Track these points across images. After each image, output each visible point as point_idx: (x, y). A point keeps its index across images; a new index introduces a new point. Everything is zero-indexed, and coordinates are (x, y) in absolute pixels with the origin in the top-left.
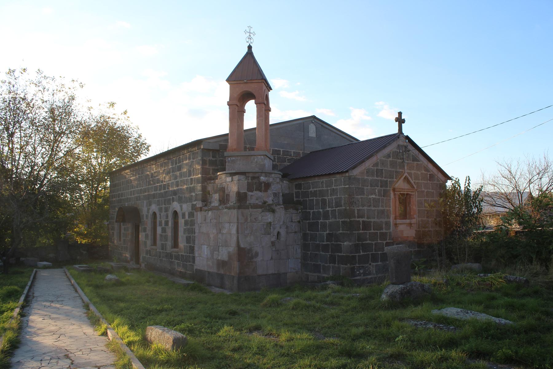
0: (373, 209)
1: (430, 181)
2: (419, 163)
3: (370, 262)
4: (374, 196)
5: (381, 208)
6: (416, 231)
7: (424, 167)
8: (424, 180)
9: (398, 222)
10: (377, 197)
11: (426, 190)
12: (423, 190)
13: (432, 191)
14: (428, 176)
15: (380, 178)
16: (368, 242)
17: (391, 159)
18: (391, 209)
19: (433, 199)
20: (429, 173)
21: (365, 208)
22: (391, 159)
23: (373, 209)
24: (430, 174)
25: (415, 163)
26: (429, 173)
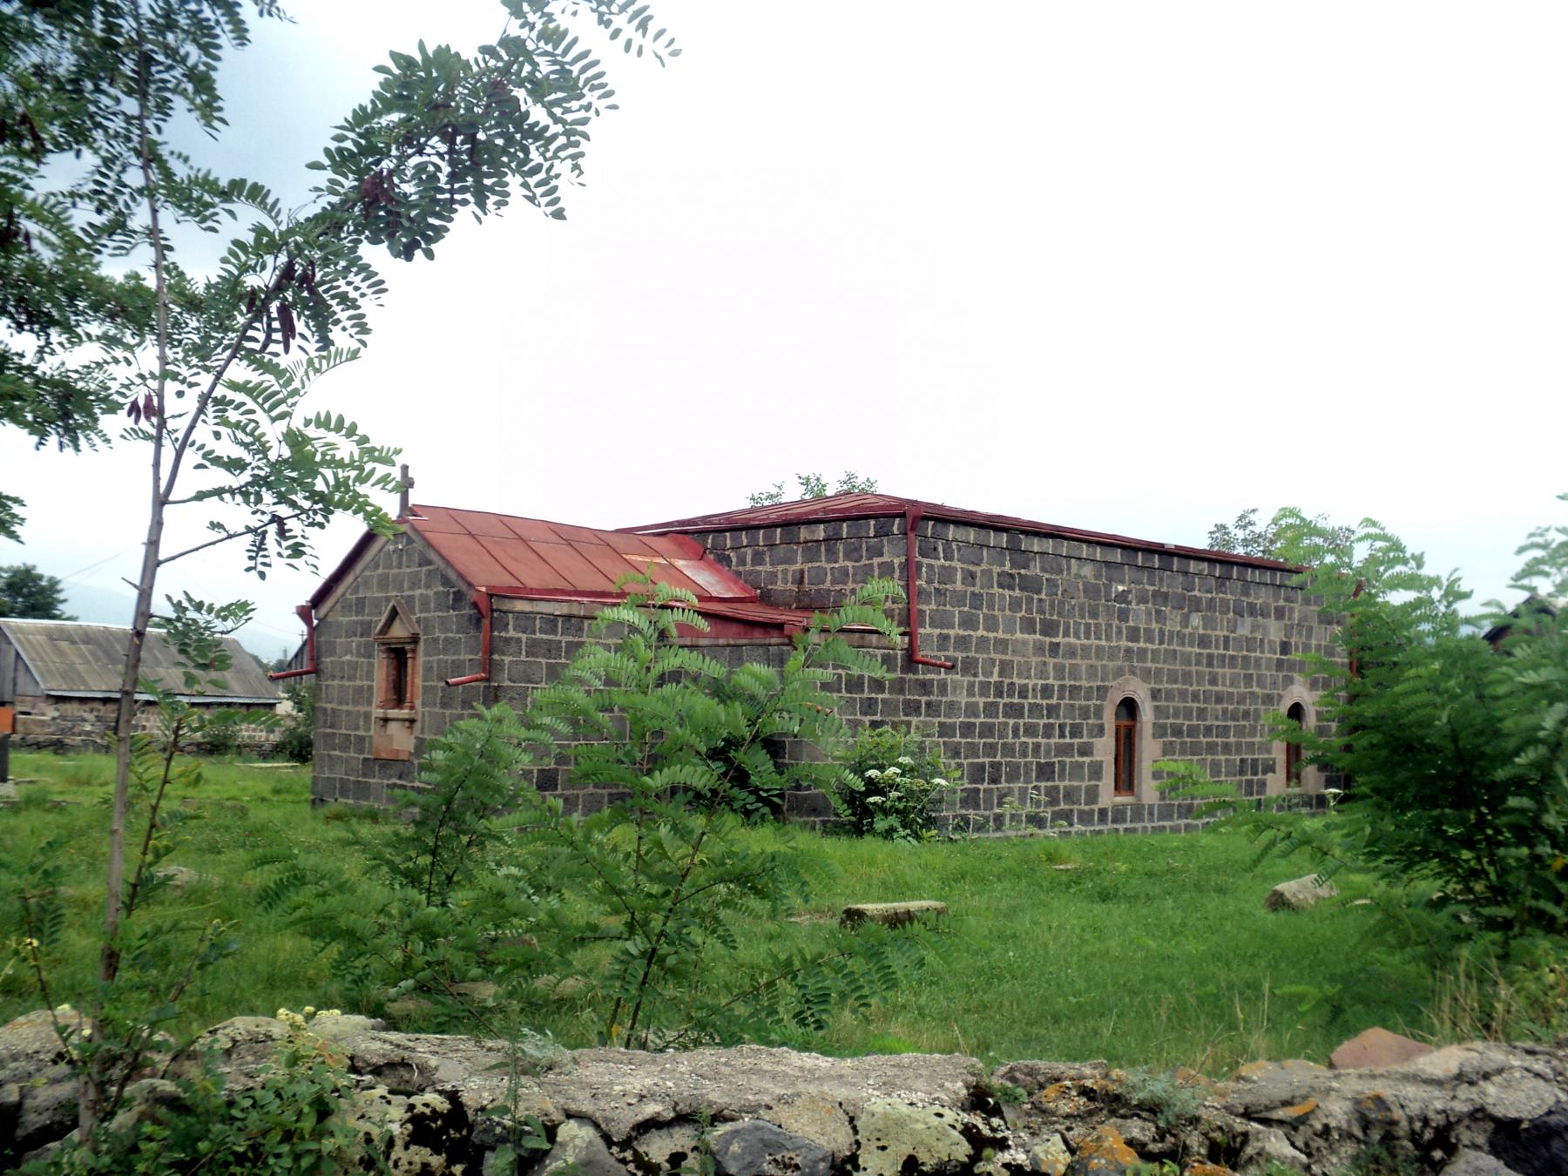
0: (347, 683)
1: (454, 610)
2: (431, 568)
3: (337, 795)
4: (348, 657)
5: (358, 683)
6: (416, 738)
7: (442, 575)
8: (440, 610)
9: (390, 716)
10: (355, 659)
11: (443, 636)
12: (437, 634)
13: (458, 636)
14: (451, 597)
15: (360, 618)
16: (337, 753)
17: (380, 571)
18: (375, 684)
19: (455, 657)
20: (452, 590)
21: (336, 682)
22: (380, 571)
23: (347, 683)
24: (454, 593)
25: (424, 569)
26: (452, 590)
